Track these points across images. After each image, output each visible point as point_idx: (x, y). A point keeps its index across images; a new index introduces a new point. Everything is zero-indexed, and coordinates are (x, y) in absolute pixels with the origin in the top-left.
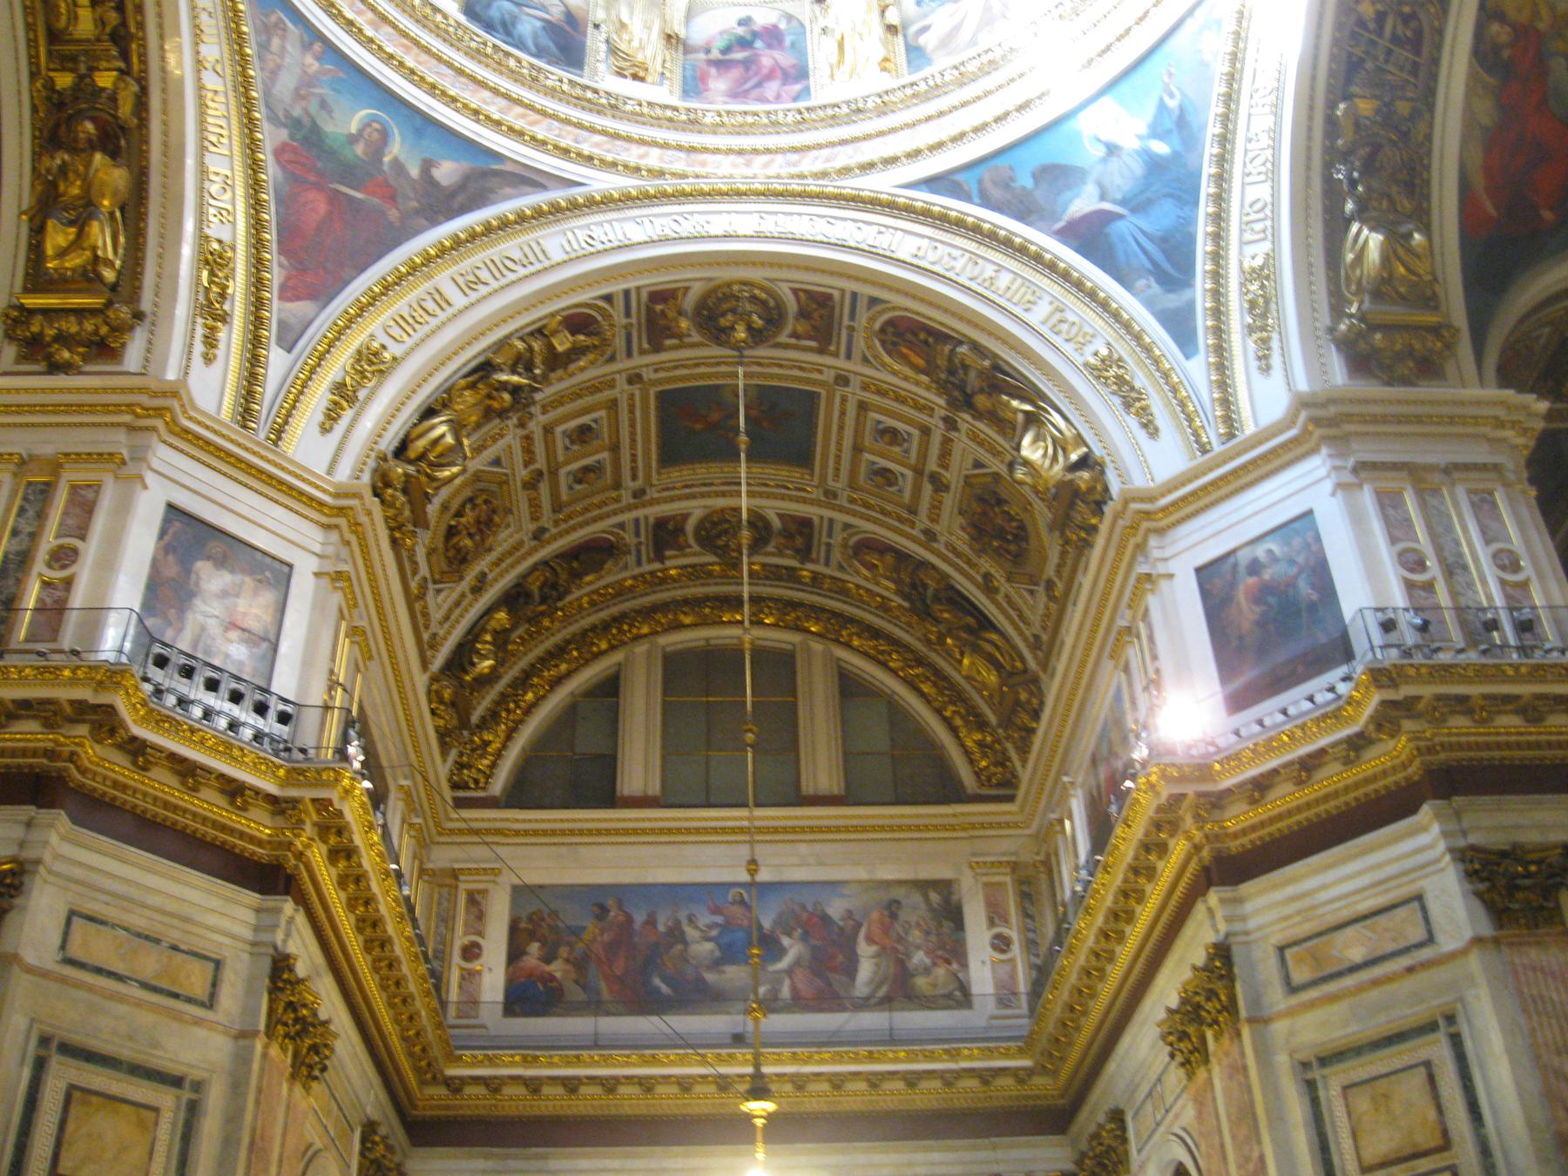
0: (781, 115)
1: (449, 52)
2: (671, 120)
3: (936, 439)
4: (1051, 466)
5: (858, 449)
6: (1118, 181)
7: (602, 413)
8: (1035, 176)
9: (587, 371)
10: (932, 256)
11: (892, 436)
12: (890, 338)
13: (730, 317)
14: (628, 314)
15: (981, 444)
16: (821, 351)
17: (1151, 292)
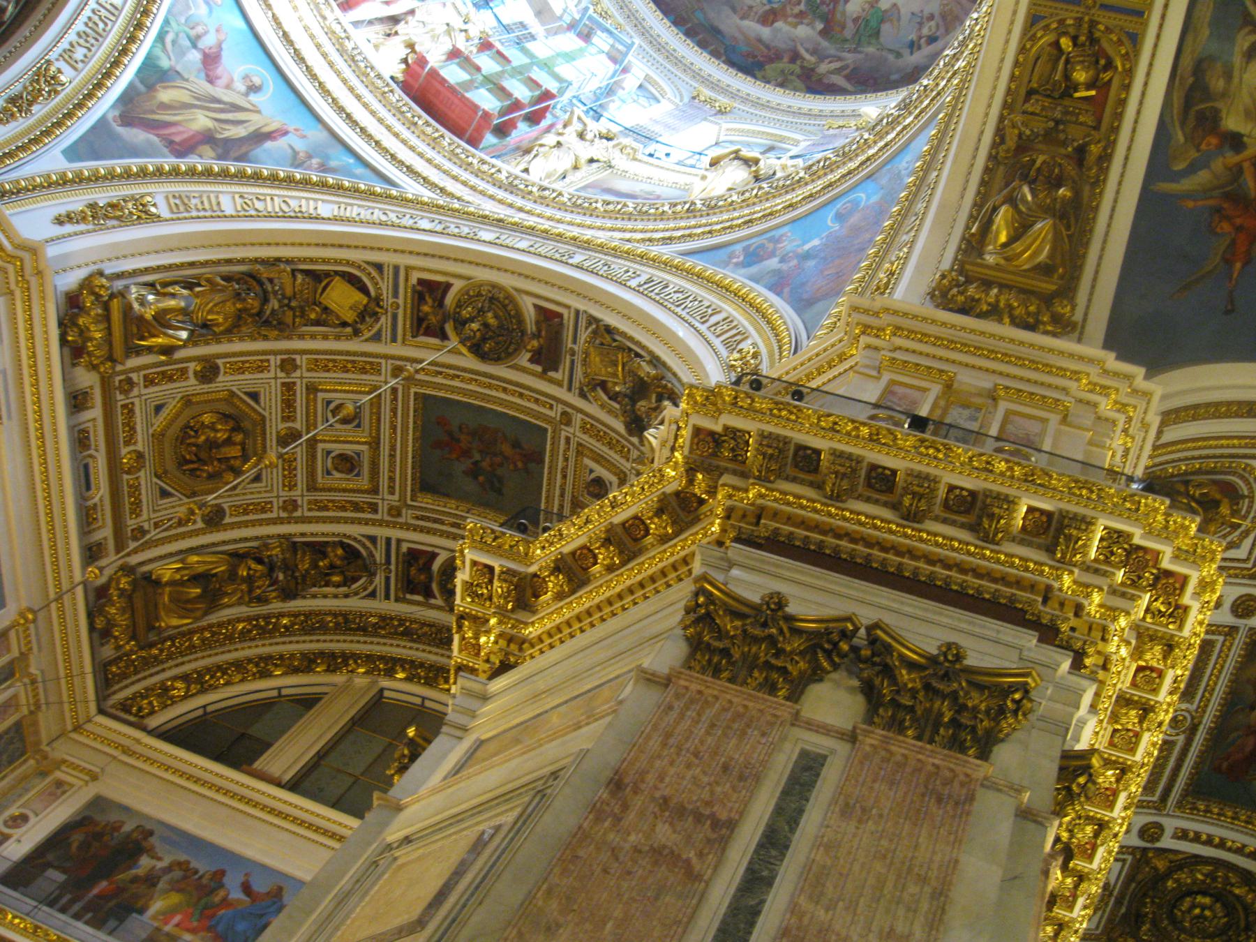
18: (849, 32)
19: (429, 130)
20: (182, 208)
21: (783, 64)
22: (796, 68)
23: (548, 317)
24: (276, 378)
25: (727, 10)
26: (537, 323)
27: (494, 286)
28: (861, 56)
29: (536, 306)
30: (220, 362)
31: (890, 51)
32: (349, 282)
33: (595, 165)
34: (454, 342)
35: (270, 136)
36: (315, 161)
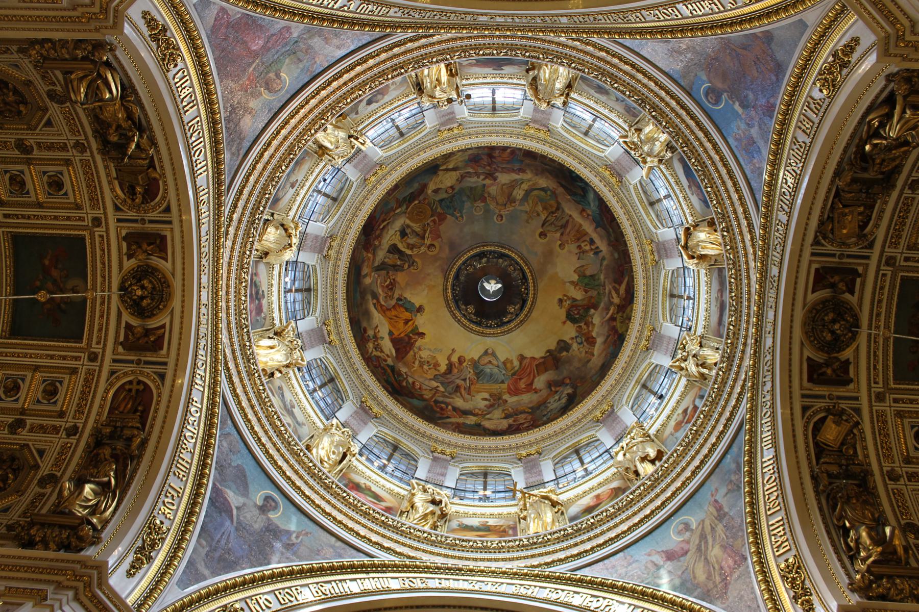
0: (244, 316)
1: (296, 133)
2: (245, 253)
3: (57, 422)
4: (81, 506)
5: (36, 368)
6: (248, 516)
7: (72, 200)
8: (238, 466)
9: (111, 192)
10: (193, 409)
11: (51, 392)
12: (134, 387)
13: (150, 286)
14: (151, 222)
15: (61, 453)
16: (116, 342)
17: (201, 549)
18: (594, 293)
19: (699, 422)
20: (787, 543)
21: (618, 324)
22: (618, 317)
23: (821, 278)
24: (906, 485)
25: (590, 365)
26: (825, 287)
27: (804, 324)
28: (607, 282)
29: (813, 292)
30: (903, 522)
31: (601, 265)
32: (819, 431)
33: (704, 342)
34: (848, 354)
35: (719, 508)
36: (733, 478)
